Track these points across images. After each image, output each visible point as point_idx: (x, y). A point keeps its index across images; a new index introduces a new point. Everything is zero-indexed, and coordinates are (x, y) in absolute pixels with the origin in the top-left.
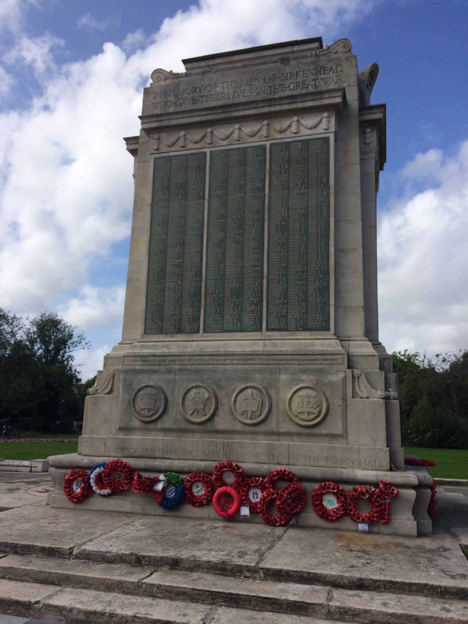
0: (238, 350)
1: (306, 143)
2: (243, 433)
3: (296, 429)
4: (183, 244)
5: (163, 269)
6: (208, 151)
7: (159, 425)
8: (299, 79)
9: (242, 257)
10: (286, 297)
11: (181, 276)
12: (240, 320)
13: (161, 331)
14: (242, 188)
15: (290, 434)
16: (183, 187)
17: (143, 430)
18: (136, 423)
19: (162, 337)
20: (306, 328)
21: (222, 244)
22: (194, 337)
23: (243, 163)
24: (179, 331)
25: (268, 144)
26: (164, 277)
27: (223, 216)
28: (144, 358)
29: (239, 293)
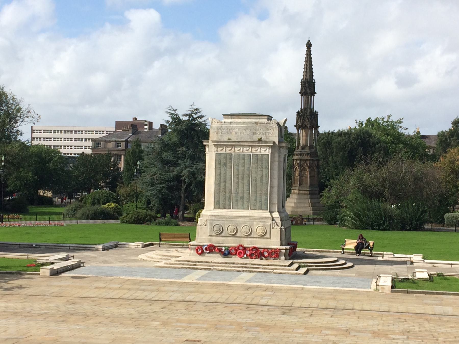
0: (242, 215)
1: (263, 155)
2: (244, 237)
3: (243, 236)
4: (225, 182)
5: (220, 189)
6: (233, 153)
7: (221, 235)
8: (261, 131)
9: (243, 188)
10: (256, 200)
11: (225, 192)
12: (243, 206)
13: (219, 208)
14: (244, 166)
15: (256, 238)
16: (225, 164)
17: (216, 236)
18: (214, 234)
19: (219, 210)
20: (261, 209)
21: (237, 183)
22: (229, 210)
23: (244, 159)
24: (225, 208)
25: (251, 154)
26: (220, 192)
27: (238, 175)
28: (215, 216)
29: (242, 198)
